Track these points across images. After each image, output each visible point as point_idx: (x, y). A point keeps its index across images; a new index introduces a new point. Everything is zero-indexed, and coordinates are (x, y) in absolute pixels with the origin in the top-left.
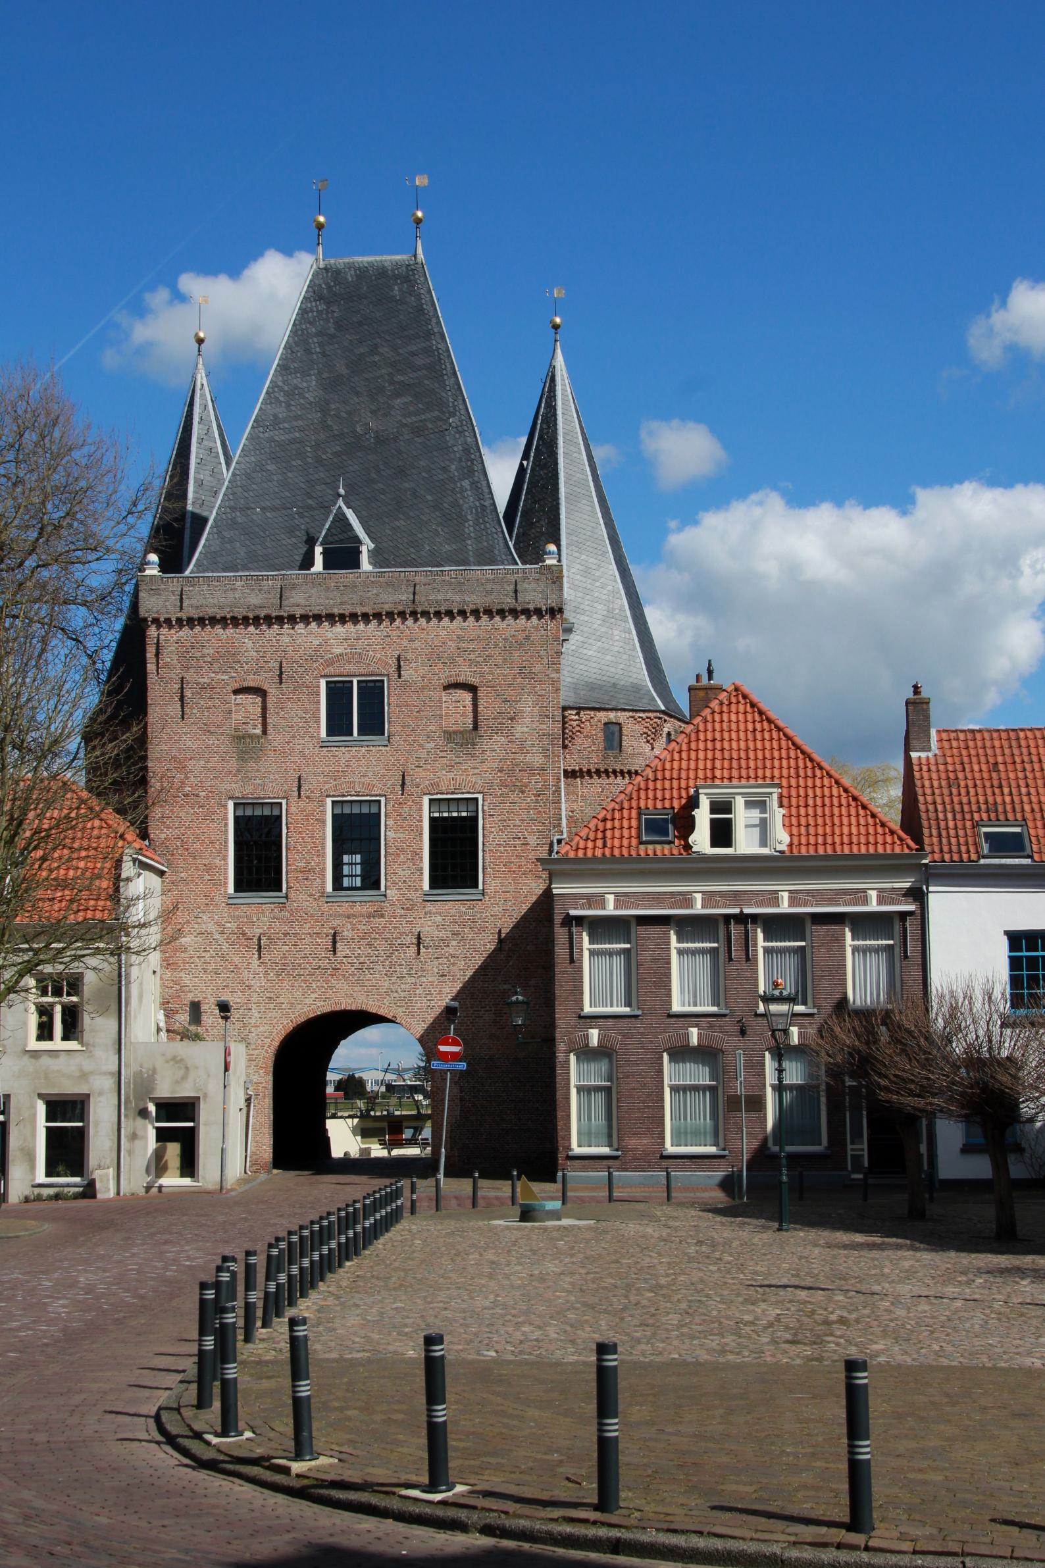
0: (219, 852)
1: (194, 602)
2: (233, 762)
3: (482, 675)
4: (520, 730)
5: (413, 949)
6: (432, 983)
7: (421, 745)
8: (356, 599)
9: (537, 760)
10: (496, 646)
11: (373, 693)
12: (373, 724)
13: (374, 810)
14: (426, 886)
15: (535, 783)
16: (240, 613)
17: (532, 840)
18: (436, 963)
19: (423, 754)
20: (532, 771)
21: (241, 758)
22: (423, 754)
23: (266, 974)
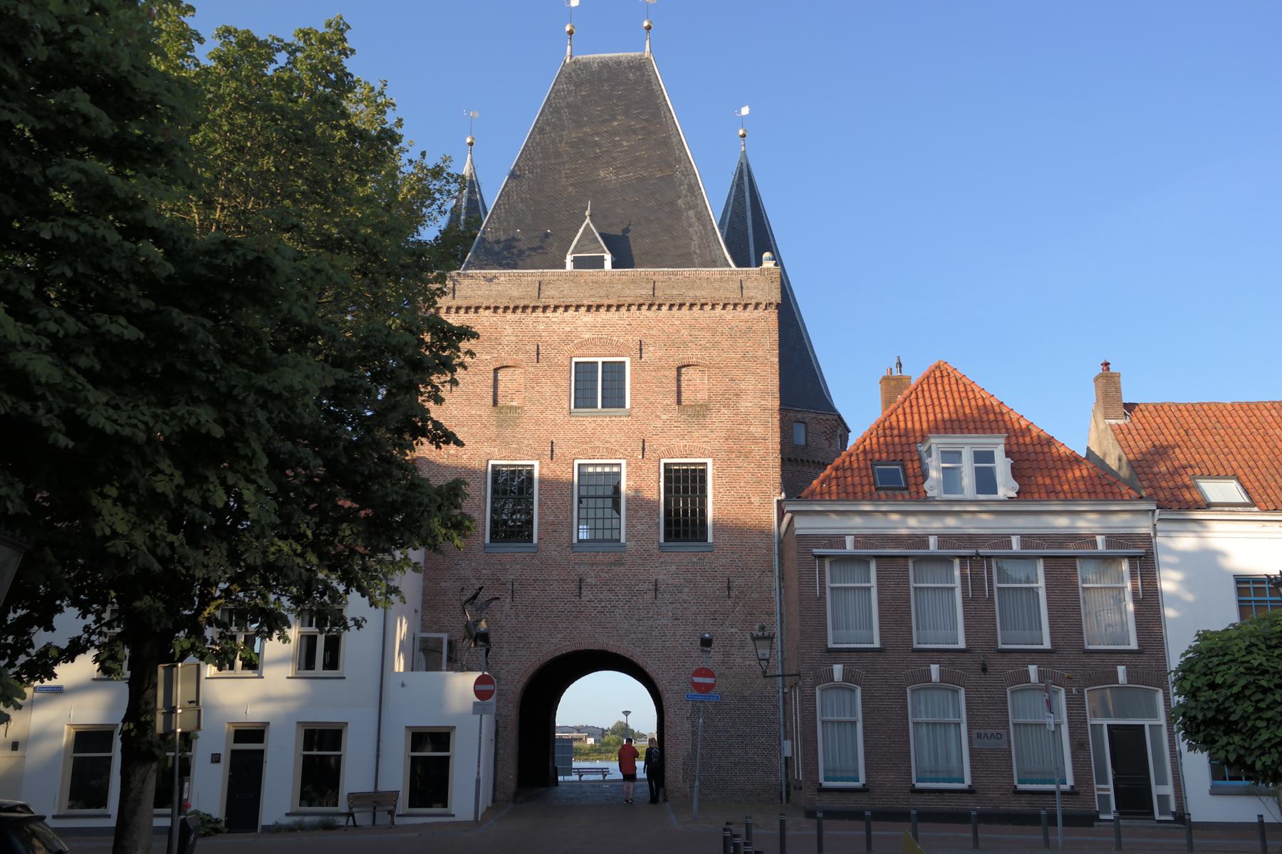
0: (479, 506)
1: (463, 293)
2: (493, 428)
3: (711, 357)
4: (746, 404)
5: (651, 594)
6: (666, 626)
7: (658, 417)
8: (603, 293)
9: (757, 430)
10: (722, 334)
11: (614, 372)
12: (614, 398)
13: (615, 469)
14: (662, 540)
15: (757, 450)
16: (503, 302)
17: (756, 500)
18: (671, 607)
19: (659, 424)
20: (755, 440)
21: (499, 426)
22: (659, 424)
23: (517, 616)
